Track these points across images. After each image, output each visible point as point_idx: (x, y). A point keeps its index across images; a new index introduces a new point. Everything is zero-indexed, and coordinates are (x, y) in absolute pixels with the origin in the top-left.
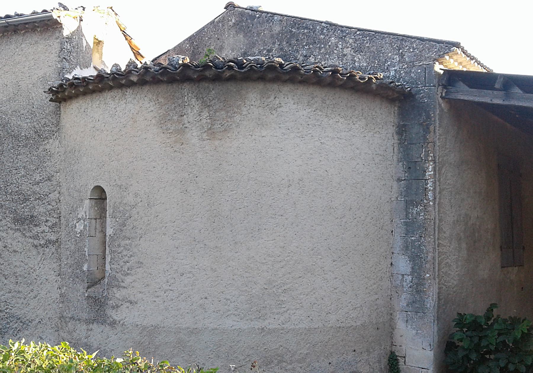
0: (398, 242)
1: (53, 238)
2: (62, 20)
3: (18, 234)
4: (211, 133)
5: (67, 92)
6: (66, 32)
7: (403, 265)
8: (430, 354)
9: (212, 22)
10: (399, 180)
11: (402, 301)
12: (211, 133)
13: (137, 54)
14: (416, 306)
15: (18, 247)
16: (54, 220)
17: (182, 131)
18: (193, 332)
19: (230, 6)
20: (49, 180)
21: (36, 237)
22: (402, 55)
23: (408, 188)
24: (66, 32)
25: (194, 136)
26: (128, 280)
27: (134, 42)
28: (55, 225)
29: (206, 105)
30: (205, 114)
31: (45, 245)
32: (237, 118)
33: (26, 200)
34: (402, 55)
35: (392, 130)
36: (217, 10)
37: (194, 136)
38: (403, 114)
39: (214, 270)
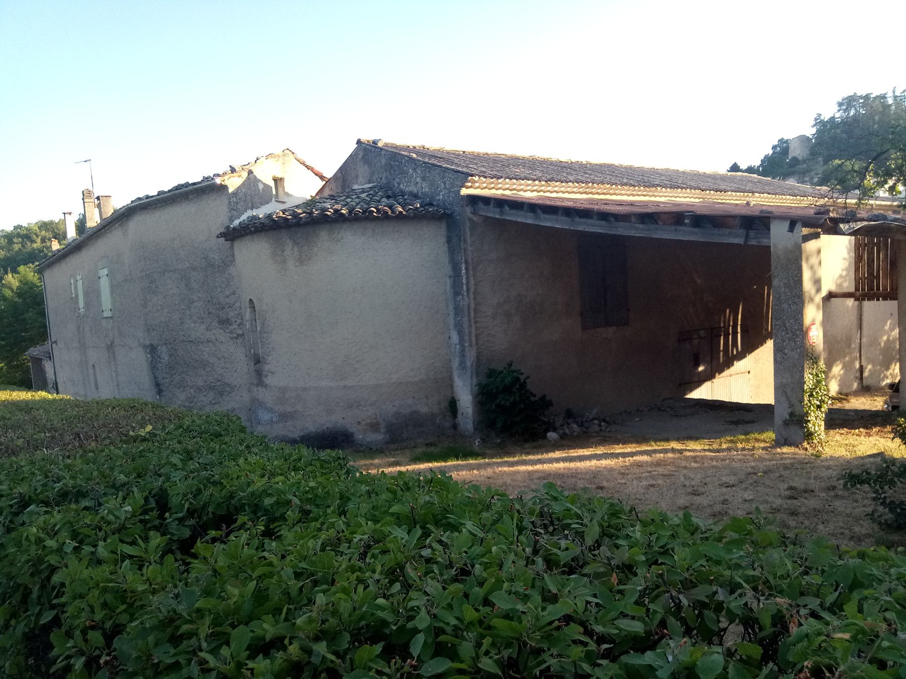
0: (451, 321)
1: (240, 332)
2: (226, 183)
3: (222, 331)
4: (301, 261)
5: (232, 235)
6: (230, 191)
7: (455, 338)
8: (470, 397)
9: (351, 155)
10: (450, 277)
11: (455, 364)
12: (301, 261)
13: (322, 177)
14: (462, 364)
15: (223, 339)
16: (239, 321)
17: (284, 262)
18: (305, 389)
19: (359, 142)
20: (234, 294)
21: (231, 332)
22: (445, 184)
23: (454, 282)
24: (230, 191)
25: (291, 264)
26: (270, 359)
27: (318, 168)
28: (240, 324)
29: (295, 243)
30: (296, 249)
31: (237, 338)
32: (315, 249)
33: (224, 308)
34: (445, 184)
35: (444, 240)
36: (351, 147)
37: (291, 264)
38: (449, 228)
39: (312, 351)
